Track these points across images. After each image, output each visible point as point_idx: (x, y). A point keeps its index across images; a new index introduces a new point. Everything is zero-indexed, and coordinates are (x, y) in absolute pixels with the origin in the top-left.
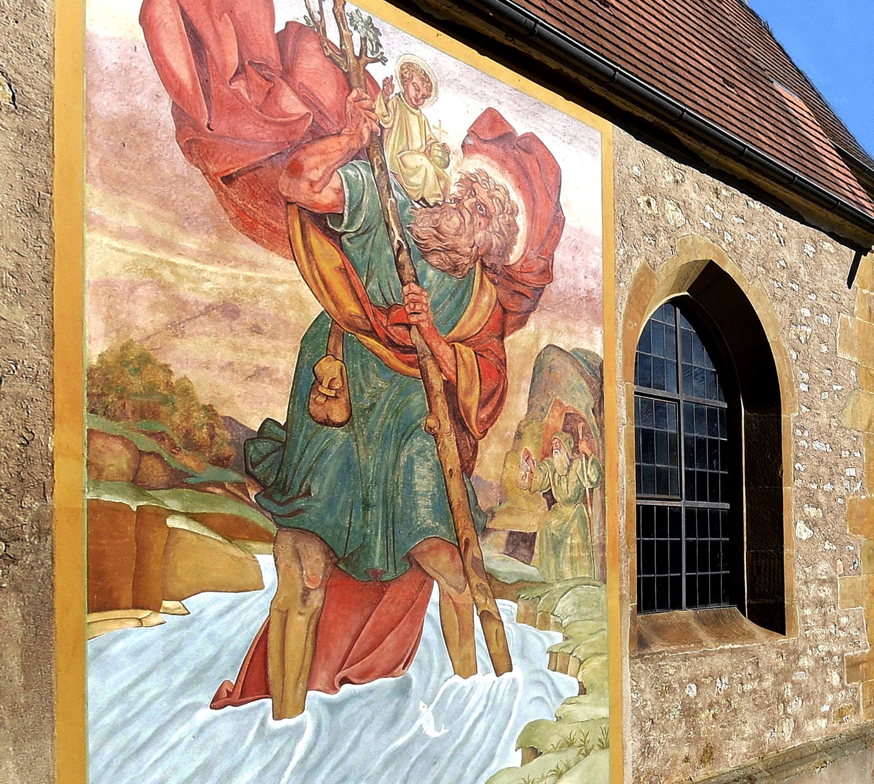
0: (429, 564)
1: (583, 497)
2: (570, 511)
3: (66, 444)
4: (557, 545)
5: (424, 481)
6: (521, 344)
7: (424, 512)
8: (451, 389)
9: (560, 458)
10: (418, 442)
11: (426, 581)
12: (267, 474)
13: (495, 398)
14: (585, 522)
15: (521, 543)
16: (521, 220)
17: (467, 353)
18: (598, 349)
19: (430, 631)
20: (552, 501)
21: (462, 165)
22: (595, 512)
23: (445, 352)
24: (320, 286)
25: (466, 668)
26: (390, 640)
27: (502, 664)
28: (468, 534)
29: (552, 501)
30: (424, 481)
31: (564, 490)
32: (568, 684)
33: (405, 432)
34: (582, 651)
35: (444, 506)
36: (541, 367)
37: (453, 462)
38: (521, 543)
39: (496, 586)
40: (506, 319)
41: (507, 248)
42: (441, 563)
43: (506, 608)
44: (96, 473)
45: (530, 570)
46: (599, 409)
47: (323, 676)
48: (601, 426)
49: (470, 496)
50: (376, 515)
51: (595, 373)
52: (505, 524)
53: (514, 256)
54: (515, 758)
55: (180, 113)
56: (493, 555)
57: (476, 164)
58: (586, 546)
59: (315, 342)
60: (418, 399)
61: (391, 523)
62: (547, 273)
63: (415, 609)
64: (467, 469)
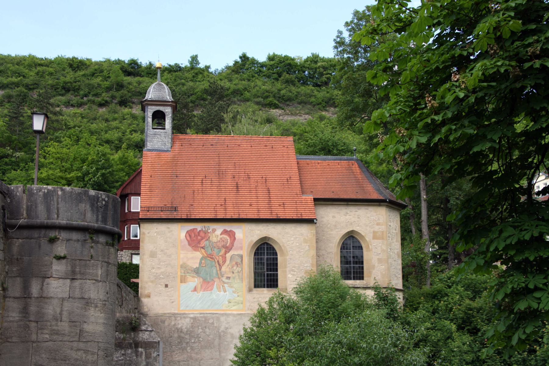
0: (215, 280)
1: (238, 272)
5: (214, 271)
6: (228, 255)
7: (214, 275)
8: (218, 261)
9: (235, 268)
11: (215, 282)
12: (197, 271)
13: (224, 261)
15: (228, 278)
17: (221, 257)
20: (233, 273)
21: (220, 237)
22: (241, 274)
23: (217, 258)
24: (202, 254)
25: (220, 291)
27: (225, 291)
28: (220, 276)
29: (233, 273)
32: (236, 295)
33: (212, 267)
37: (218, 268)
38: (228, 278)
39: (224, 283)
40: (226, 253)
42: (217, 280)
43: (225, 285)
44: (181, 273)
48: (242, 263)
49: (221, 273)
52: (226, 275)
53: (228, 245)
54: (227, 303)
56: (224, 279)
57: (222, 236)
60: (214, 263)
61: (210, 276)
62: (233, 246)
63: (213, 284)
64: (220, 269)
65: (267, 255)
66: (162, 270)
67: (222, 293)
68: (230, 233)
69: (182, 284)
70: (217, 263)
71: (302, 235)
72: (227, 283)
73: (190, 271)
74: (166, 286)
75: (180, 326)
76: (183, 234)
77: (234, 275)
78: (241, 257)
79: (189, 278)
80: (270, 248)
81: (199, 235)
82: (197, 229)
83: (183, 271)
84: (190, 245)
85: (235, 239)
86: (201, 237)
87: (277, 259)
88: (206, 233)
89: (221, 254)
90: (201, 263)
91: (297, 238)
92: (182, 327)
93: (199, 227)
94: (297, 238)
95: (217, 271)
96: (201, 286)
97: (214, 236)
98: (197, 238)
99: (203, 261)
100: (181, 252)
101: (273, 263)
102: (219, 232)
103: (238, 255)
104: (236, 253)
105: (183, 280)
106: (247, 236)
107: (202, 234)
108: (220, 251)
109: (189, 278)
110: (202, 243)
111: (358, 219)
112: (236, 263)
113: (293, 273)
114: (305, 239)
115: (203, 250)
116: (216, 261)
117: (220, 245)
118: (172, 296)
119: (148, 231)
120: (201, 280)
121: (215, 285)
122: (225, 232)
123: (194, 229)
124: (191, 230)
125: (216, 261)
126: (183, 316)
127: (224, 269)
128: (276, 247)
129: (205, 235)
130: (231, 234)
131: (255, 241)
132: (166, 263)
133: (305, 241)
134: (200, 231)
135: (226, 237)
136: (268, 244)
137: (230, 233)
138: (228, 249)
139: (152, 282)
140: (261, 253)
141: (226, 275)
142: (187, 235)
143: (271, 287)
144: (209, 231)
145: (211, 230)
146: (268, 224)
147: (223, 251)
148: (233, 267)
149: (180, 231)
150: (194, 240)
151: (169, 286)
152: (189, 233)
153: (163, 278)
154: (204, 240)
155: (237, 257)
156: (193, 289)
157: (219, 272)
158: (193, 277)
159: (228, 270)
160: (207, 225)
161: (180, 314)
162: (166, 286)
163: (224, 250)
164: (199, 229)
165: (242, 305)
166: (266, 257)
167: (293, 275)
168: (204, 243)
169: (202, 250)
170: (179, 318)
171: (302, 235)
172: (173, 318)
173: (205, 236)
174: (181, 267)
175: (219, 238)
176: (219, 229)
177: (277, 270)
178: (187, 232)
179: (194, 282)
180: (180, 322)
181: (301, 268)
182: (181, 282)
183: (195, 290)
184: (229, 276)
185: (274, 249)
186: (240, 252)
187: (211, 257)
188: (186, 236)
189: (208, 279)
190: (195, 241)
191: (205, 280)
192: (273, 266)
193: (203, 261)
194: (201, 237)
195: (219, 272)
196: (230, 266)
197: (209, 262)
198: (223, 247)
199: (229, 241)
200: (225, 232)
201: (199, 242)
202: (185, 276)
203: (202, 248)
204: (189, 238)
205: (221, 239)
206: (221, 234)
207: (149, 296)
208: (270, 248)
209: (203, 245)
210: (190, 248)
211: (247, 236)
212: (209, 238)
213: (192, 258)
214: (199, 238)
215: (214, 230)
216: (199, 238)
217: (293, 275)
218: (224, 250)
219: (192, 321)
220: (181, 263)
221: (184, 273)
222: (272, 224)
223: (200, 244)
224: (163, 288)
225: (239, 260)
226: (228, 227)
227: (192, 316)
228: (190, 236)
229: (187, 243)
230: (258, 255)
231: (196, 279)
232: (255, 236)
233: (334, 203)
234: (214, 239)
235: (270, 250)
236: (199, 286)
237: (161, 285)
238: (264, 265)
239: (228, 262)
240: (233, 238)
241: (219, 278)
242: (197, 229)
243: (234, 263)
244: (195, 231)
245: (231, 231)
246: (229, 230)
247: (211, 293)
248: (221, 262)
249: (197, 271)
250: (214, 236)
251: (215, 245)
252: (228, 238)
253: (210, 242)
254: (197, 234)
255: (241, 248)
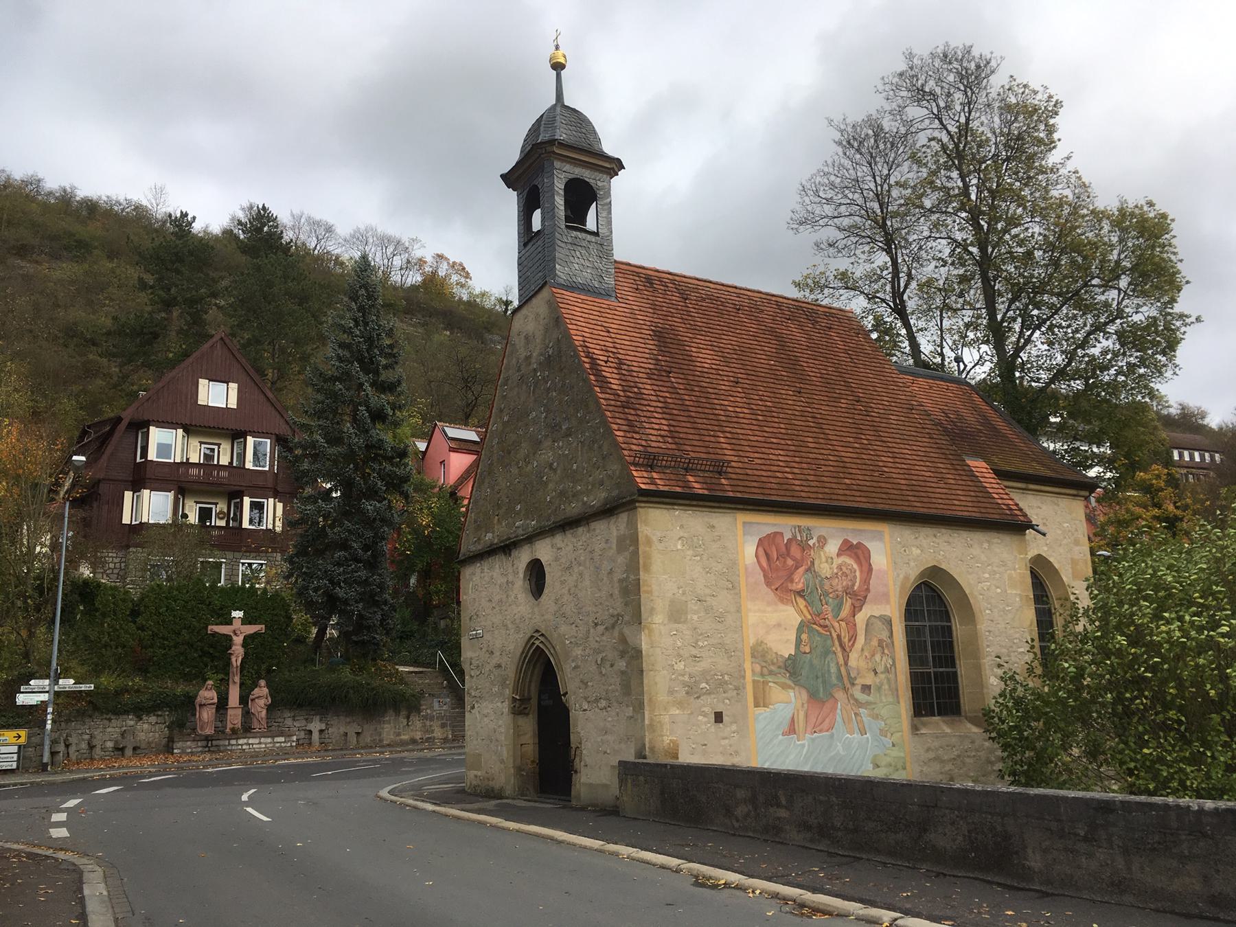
0: (836, 695)
1: (887, 671)
2: (883, 676)
3: (748, 665)
4: (879, 688)
5: (833, 670)
6: (861, 618)
7: (834, 680)
8: (839, 637)
9: (878, 657)
10: (830, 656)
11: (836, 701)
13: (853, 638)
14: (888, 680)
16: (858, 574)
17: (843, 624)
18: (888, 613)
19: (839, 719)
20: (876, 673)
22: (892, 676)
23: (836, 625)
24: (800, 612)
26: (827, 721)
27: (863, 732)
28: (848, 685)
29: (876, 673)
30: (833, 670)
31: (880, 669)
32: (888, 741)
34: (892, 730)
35: (840, 677)
36: (868, 624)
37: (841, 661)
38: (866, 688)
39: (859, 704)
40: (855, 610)
41: (853, 585)
42: (840, 695)
45: (870, 699)
46: (891, 636)
47: (809, 729)
50: (820, 680)
51: (888, 622)
52: (859, 681)
55: (765, 576)
58: (890, 689)
59: (800, 630)
60: (829, 642)
61: (824, 682)
62: (868, 590)
63: (834, 709)
64: (846, 664)
66: (704, 665)
67: (856, 736)
68: (860, 552)
70: (837, 643)
73: (772, 668)
74: (719, 717)
76: (749, 550)
78: (888, 622)
81: (788, 554)
82: (782, 534)
83: (758, 668)
84: (768, 584)
85: (870, 569)
86: (794, 559)
90: (799, 642)
93: (786, 525)
96: (806, 716)
99: (804, 636)
102: (833, 547)
107: (795, 551)
108: (839, 607)
110: (796, 577)
112: (880, 642)
118: (737, 753)
119: (659, 534)
120: (805, 695)
123: (776, 533)
124: (768, 535)
127: (855, 659)
131: (912, 578)
132: (712, 641)
138: (859, 600)
139: (680, 704)
142: (761, 549)
144: (811, 542)
148: (873, 655)
149: (742, 538)
151: (725, 718)
152: (765, 544)
153: (709, 693)
154: (801, 570)
156: (786, 727)
158: (784, 687)
159: (863, 664)
162: (719, 717)
166: (927, 624)
168: (799, 581)
169: (800, 600)
173: (803, 560)
175: (835, 566)
183: (792, 729)
188: (757, 556)
191: (813, 696)
194: (794, 559)
195: (843, 670)
199: (858, 574)
202: (765, 683)
203: (800, 593)
204: (764, 564)
205: (840, 567)
206: (838, 555)
209: (800, 586)
212: (813, 563)
215: (822, 541)
220: (752, 641)
221: (762, 675)
223: (792, 581)
225: (884, 635)
233: (1043, 488)
234: (824, 569)
236: (802, 714)
238: (926, 651)
239: (861, 639)
240: (865, 568)
241: (845, 690)
242: (782, 534)
243: (875, 643)
247: (832, 736)
249: (792, 668)
252: (855, 566)
253: (816, 575)
254: (784, 549)
255: (885, 598)
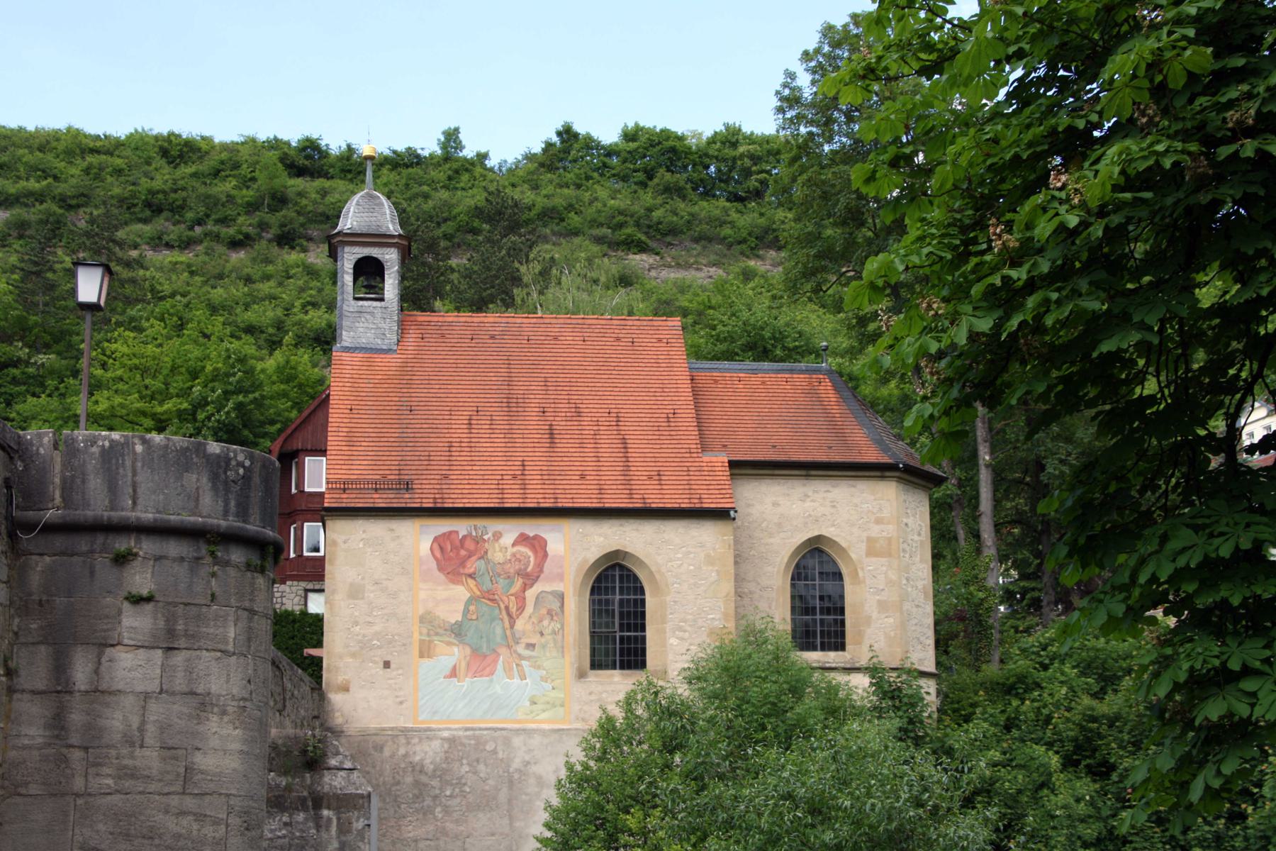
0: (500, 651)
1: (554, 633)
5: (499, 631)
6: (531, 594)
7: (498, 639)
8: (507, 608)
9: (545, 623)
11: (499, 655)
12: (457, 631)
13: (521, 608)
17: (513, 598)
20: (542, 634)
21: (511, 550)
22: (559, 637)
23: (505, 599)
24: (470, 590)
27: (523, 677)
28: (511, 643)
29: (542, 634)
32: (548, 686)
33: (493, 620)
37: (507, 624)
38: (531, 646)
39: (521, 657)
40: (525, 588)
42: (503, 651)
43: (524, 663)
44: (421, 634)
48: (563, 612)
49: (513, 635)
52: (525, 640)
54: (528, 703)
56: (521, 649)
57: (515, 549)
60: (497, 611)
61: (488, 641)
62: (541, 571)
63: (495, 661)
64: (512, 627)
65: (621, 593)
66: (377, 628)
67: (517, 681)
68: (536, 542)
69: (422, 660)
70: (504, 612)
71: (702, 545)
72: (528, 658)
73: (441, 631)
74: (387, 665)
75: (417, 758)
76: (425, 545)
77: (543, 640)
78: (561, 597)
79: (439, 646)
80: (628, 576)
81: (462, 547)
82: (457, 532)
83: (425, 631)
84: (441, 569)
85: (546, 555)
86: (467, 550)
87: (643, 601)
88: (478, 541)
89: (513, 591)
90: (466, 611)
91: (690, 553)
92: (422, 760)
93: (462, 527)
94: (690, 553)
95: (504, 630)
96: (468, 665)
97: (497, 549)
98: (458, 554)
99: (472, 608)
100: (421, 585)
101: (636, 613)
102: (508, 539)
103: (553, 593)
104: (548, 588)
105: (426, 651)
106: (575, 548)
107: (470, 545)
108: (511, 585)
109: (439, 646)
110: (469, 564)
111: (832, 510)
112: (550, 612)
113: (681, 634)
114: (708, 556)
115: (471, 582)
116: (502, 606)
117: (512, 571)
118: (400, 689)
120: (468, 651)
121: (500, 662)
122: (523, 539)
123: (451, 532)
124: (444, 534)
125: (502, 606)
126: (426, 734)
127: (520, 624)
128: (641, 575)
129: (477, 546)
130: (538, 545)
131: (592, 561)
132: (385, 611)
133: (710, 560)
134: (464, 537)
135: (525, 550)
136: (622, 567)
137: (536, 542)
138: (530, 579)
139: (353, 655)
140: (607, 588)
141: (525, 640)
142: (436, 546)
143: (629, 668)
144: (486, 537)
145: (490, 535)
146: (623, 521)
147: (519, 583)
148: (541, 621)
149: (418, 538)
150: (450, 559)
151: (392, 666)
152: (440, 542)
153: (380, 647)
154: (473, 558)
155: (550, 597)
156: (447, 672)
157: (508, 632)
158: (449, 644)
159: (529, 627)
160: (480, 523)
161: (419, 730)
162: (387, 665)
163: (521, 581)
164: (462, 533)
165: (561, 710)
166: (618, 597)
167: (682, 639)
168: (474, 565)
169: (470, 581)
170: (416, 740)
171: (702, 545)
172: (403, 740)
173: (476, 550)
174: (421, 622)
175: (509, 554)
176: (508, 532)
177: (643, 628)
178: (436, 539)
179: (450, 655)
180: (418, 748)
181: (700, 622)
182: (421, 656)
183: (453, 673)
184: (533, 641)
185: (636, 579)
186: (559, 587)
187: (490, 596)
188: (431, 549)
189: (484, 650)
190: (452, 561)
191: (476, 652)
192: (635, 617)
193: (472, 608)
194: (467, 550)
195: (508, 632)
196: (534, 620)
197: (485, 609)
198: (519, 573)
199: (532, 559)
200: (523, 539)
201: (463, 563)
202: (430, 642)
203: (471, 576)
204: (438, 554)
205: (514, 555)
206: (514, 545)
207: (345, 689)
208: (628, 576)
209: (472, 570)
210: (442, 577)
211: (575, 548)
212: (486, 553)
213: (447, 600)
214: (463, 553)
215: (497, 536)
216: (463, 553)
217: (682, 639)
218: (521, 581)
219: (446, 746)
220: (421, 611)
221: (428, 635)
222: (632, 521)
223: (464, 567)
224: (379, 669)
225: (555, 606)
226: (531, 527)
227: (446, 734)
228: (441, 548)
229: (434, 564)
230: (600, 594)
231: (456, 649)
232: (593, 549)
233: (777, 472)
234: (497, 556)
235: (628, 581)
236: (463, 664)
237: (375, 662)
238: (613, 617)
239: (529, 609)
240: (541, 554)
241: (509, 647)
242: (457, 532)
243: (544, 611)
244: (453, 536)
245: (536, 537)
246: (531, 535)
247: (491, 681)
248: (513, 610)
249: (457, 631)
250: (497, 549)
251: (499, 570)
252: (530, 553)
253: (488, 562)
254: (458, 543)
255: (561, 577)
